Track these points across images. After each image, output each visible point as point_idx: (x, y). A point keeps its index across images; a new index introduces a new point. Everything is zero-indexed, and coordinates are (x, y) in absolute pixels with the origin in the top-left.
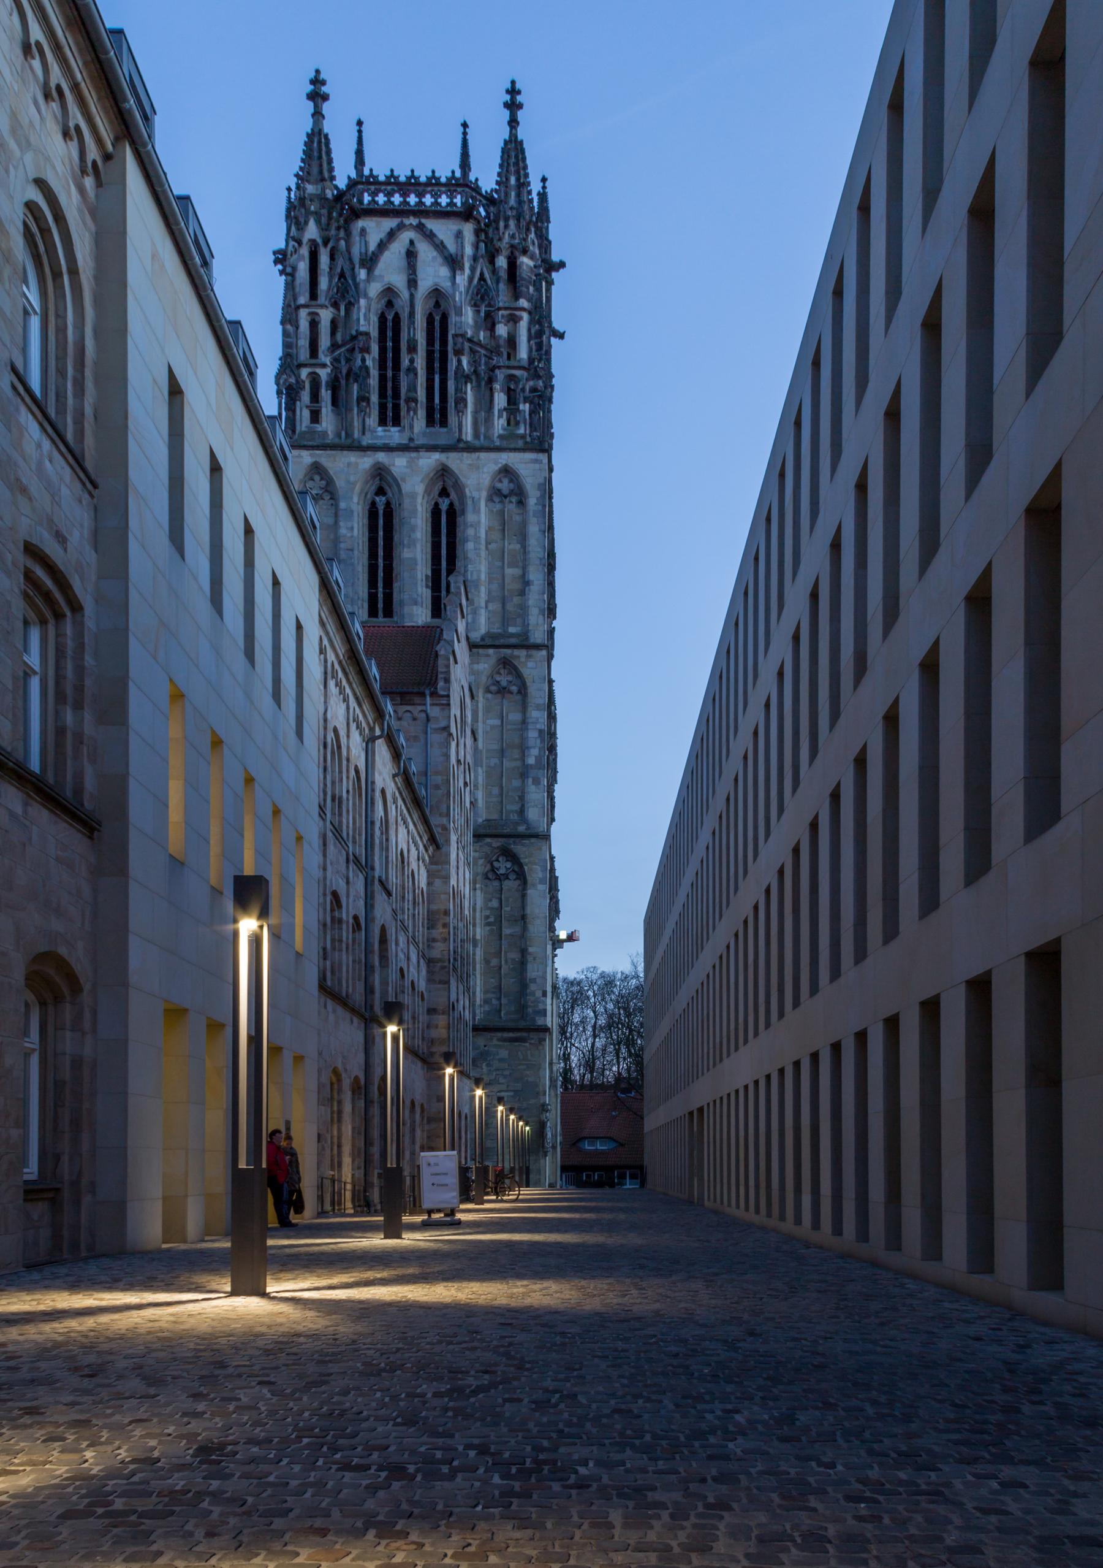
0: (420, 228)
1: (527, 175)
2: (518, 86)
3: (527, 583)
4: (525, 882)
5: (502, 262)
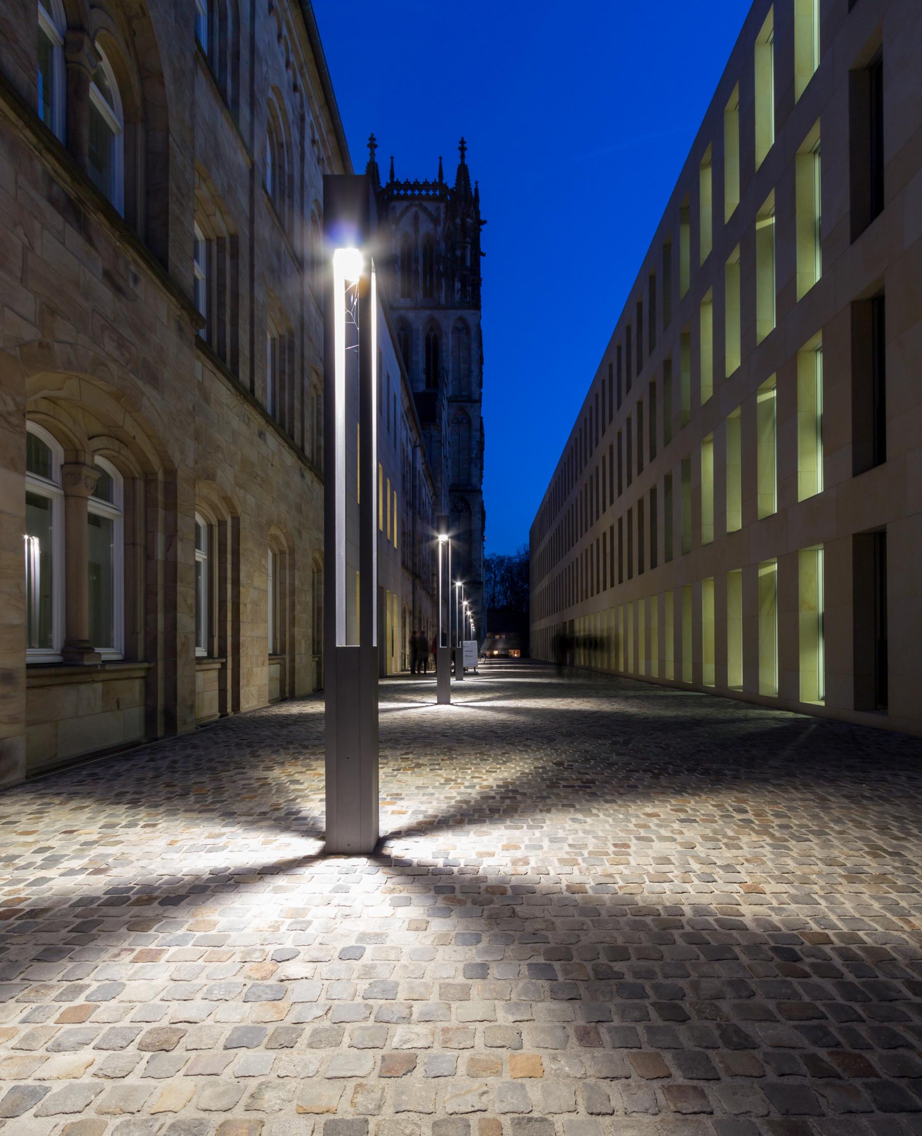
0: (421, 206)
1: (469, 181)
2: (465, 140)
3: (470, 372)
4: (471, 513)
5: (458, 221)
